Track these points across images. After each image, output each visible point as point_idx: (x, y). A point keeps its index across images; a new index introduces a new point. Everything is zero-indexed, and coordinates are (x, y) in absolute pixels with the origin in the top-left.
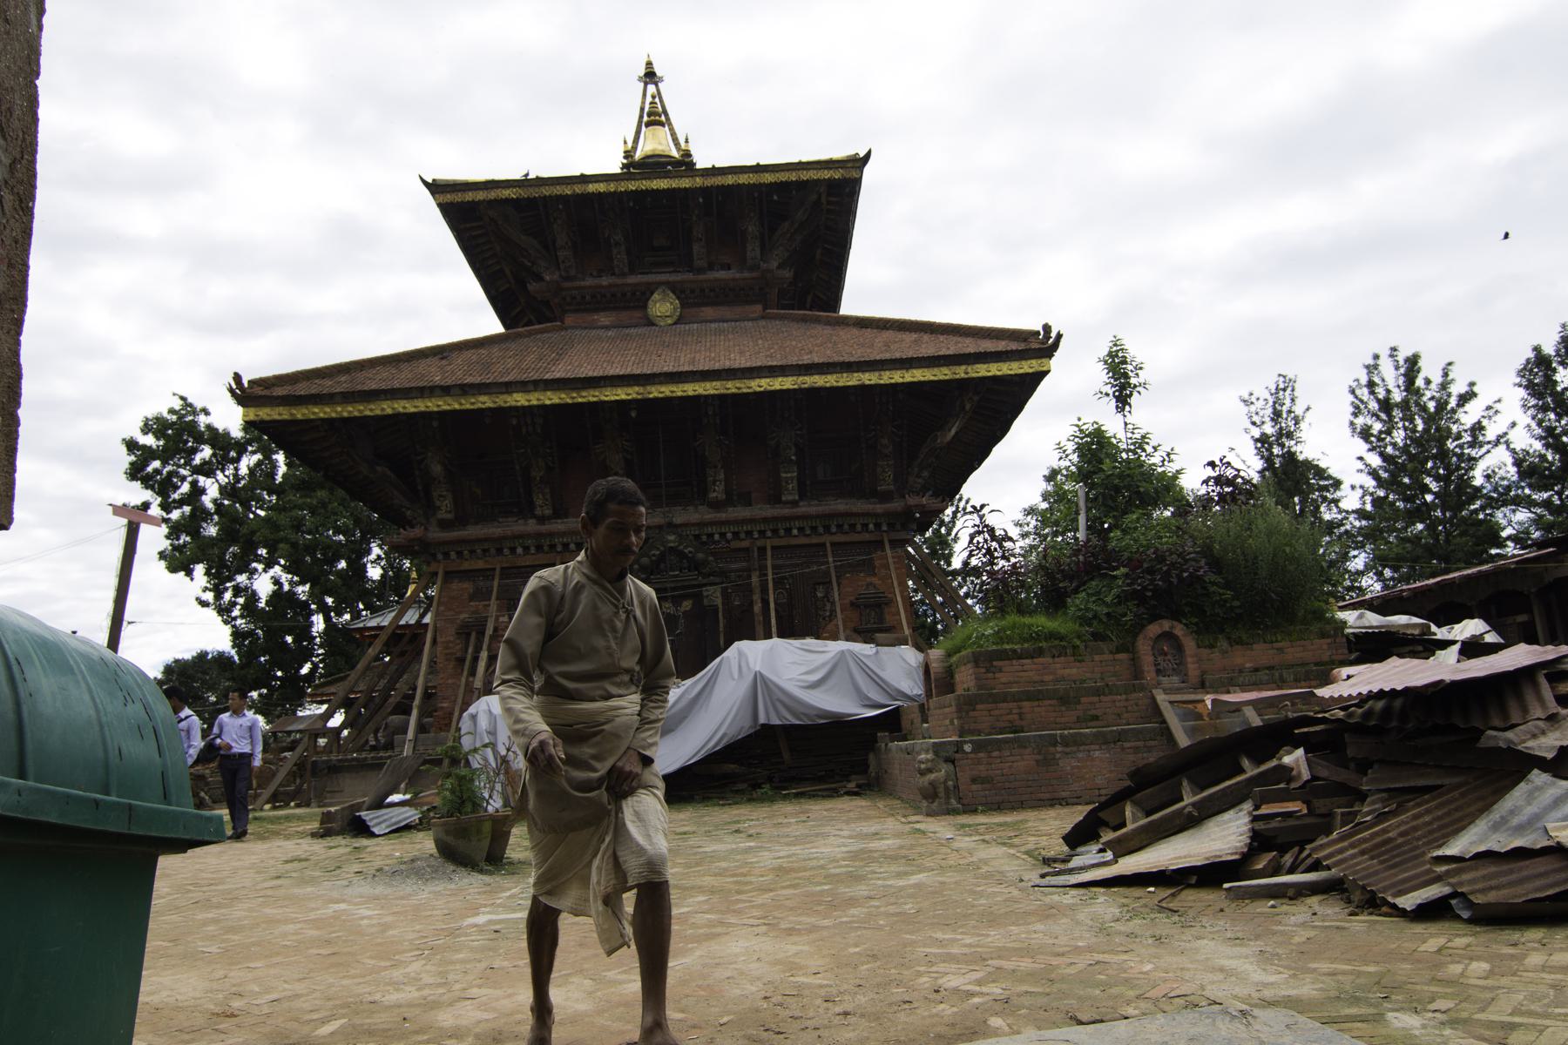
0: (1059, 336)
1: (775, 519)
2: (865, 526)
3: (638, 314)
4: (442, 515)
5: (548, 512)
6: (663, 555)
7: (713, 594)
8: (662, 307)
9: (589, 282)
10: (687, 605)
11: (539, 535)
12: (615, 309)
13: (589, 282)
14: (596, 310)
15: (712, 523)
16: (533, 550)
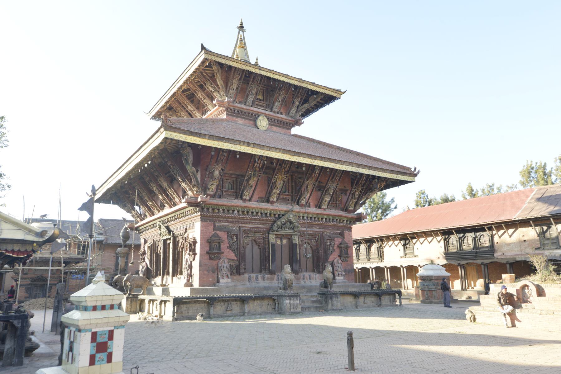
0: (419, 172)
1: (321, 214)
2: (343, 221)
3: (252, 122)
4: (209, 192)
5: (248, 198)
6: (286, 222)
7: (296, 240)
8: (263, 122)
9: (237, 105)
10: (285, 241)
11: (245, 207)
12: (244, 118)
13: (237, 105)
14: (237, 117)
15: (302, 212)
16: (241, 213)
